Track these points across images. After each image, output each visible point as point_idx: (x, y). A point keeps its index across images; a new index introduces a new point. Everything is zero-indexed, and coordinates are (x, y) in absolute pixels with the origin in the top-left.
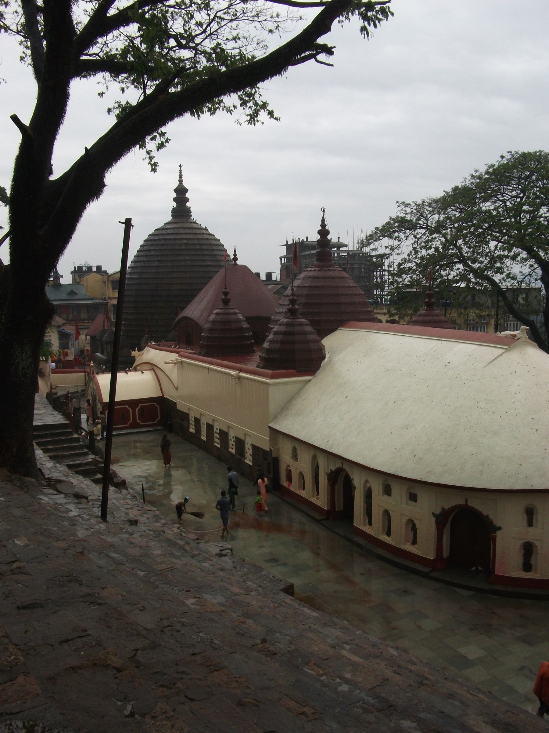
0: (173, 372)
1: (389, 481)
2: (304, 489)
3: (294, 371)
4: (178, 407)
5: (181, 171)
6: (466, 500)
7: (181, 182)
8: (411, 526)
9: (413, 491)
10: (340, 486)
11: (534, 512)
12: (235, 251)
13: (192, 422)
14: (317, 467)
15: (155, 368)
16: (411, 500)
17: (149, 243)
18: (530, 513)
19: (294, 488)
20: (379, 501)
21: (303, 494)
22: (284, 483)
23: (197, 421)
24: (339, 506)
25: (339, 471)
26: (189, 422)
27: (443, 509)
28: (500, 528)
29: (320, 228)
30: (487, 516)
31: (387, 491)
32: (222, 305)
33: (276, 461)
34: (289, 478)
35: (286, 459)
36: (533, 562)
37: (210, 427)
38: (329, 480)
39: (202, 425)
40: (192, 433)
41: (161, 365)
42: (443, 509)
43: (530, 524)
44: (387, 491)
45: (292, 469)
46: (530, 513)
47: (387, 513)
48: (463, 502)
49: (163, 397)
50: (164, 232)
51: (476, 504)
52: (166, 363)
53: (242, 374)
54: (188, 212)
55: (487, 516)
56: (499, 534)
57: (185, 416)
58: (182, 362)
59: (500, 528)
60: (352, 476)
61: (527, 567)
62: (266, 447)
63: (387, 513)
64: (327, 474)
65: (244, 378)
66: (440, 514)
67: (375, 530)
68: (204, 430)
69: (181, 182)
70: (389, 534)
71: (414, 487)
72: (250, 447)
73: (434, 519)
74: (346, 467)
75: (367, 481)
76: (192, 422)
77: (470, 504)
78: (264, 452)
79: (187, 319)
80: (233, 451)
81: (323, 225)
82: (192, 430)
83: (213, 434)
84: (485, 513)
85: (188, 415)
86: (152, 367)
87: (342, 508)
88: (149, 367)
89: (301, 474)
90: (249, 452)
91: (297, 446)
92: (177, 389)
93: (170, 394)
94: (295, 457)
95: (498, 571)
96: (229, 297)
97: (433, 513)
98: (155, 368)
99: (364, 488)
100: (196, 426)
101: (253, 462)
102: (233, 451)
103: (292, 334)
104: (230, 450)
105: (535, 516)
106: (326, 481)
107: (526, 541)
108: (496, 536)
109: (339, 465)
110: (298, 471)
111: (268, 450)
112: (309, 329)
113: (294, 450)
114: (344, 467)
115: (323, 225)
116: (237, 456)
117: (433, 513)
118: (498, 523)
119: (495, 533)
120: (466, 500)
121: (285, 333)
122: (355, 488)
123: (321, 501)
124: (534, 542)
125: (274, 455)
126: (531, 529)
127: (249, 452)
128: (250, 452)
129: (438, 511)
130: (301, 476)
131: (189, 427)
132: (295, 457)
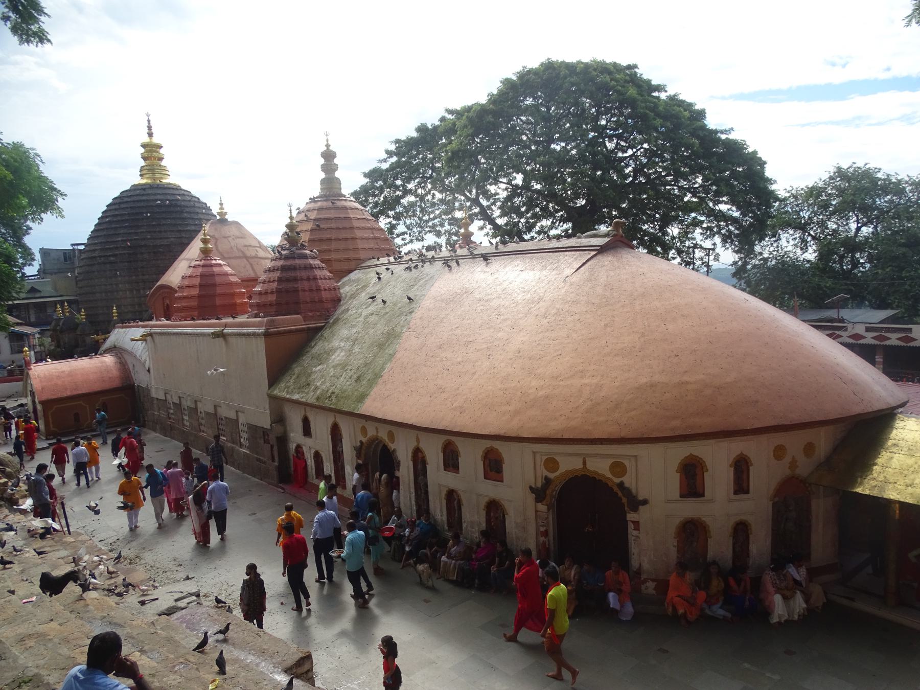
0: (139, 348)
1: (451, 444)
5: (149, 121)
6: (584, 463)
17: (114, 207)
28: (645, 502)
31: (451, 462)
33: (283, 440)
35: (296, 436)
44: (451, 462)
48: (579, 465)
58: (151, 334)
59: (645, 502)
60: (392, 446)
63: (452, 498)
72: (245, 429)
78: (265, 433)
79: (163, 287)
91: (311, 418)
93: (141, 379)
94: (307, 432)
97: (531, 488)
103: (294, 268)
109: (371, 432)
110: (313, 451)
111: (269, 427)
113: (306, 423)
114: (379, 435)
117: (531, 488)
120: (584, 463)
121: (283, 269)
130: (317, 456)
132: (307, 432)
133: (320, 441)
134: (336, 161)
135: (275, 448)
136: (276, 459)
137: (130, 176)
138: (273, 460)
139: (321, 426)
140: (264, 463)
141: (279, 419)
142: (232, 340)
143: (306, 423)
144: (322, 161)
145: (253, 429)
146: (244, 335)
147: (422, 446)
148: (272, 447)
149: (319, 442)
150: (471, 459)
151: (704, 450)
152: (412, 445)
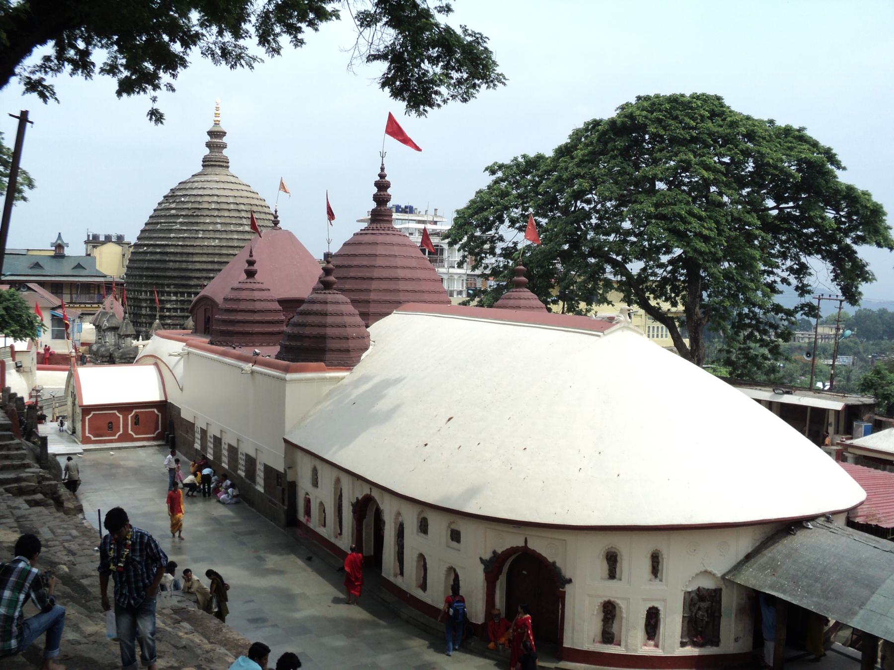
2: (324, 526)
4: (183, 415)
7: (217, 124)
8: (453, 576)
9: (454, 527)
10: (369, 520)
11: (618, 559)
13: (198, 436)
16: (452, 540)
18: (612, 559)
19: (314, 524)
20: (413, 542)
21: (322, 531)
22: (302, 517)
23: (204, 432)
24: (368, 549)
26: (194, 436)
27: (494, 552)
28: (570, 581)
29: (378, 178)
30: (554, 563)
31: (423, 527)
34: (308, 512)
35: (304, 485)
36: (615, 628)
37: (218, 441)
38: (354, 512)
39: (209, 439)
41: (165, 358)
42: (494, 552)
43: (612, 575)
44: (423, 527)
46: (612, 559)
47: (422, 557)
49: (166, 401)
51: (539, 545)
52: (170, 355)
54: (224, 164)
55: (554, 563)
56: (568, 588)
57: (190, 426)
59: (570, 581)
60: (382, 507)
61: (608, 637)
62: (280, 467)
64: (352, 505)
65: (258, 372)
66: (491, 559)
67: (408, 582)
70: (424, 587)
71: (457, 521)
72: (262, 468)
73: (482, 567)
74: (376, 494)
75: (399, 514)
76: (198, 436)
77: (532, 545)
78: (278, 473)
79: (205, 298)
80: (243, 474)
81: (382, 176)
82: (197, 446)
83: (221, 450)
84: (551, 560)
85: (193, 424)
86: (155, 360)
87: (372, 554)
88: (153, 360)
89: (321, 504)
91: (319, 468)
92: (181, 389)
95: (567, 644)
96: (256, 267)
97: (481, 559)
98: (159, 362)
99: (395, 523)
100: (201, 439)
101: (265, 488)
102: (243, 474)
105: (618, 565)
107: (606, 599)
108: (564, 592)
109: (366, 490)
110: (318, 501)
111: (282, 471)
112: (350, 308)
113: (315, 471)
115: (382, 176)
116: (248, 481)
117: (481, 559)
118: (567, 573)
119: (563, 587)
122: (384, 523)
123: (345, 543)
124: (618, 601)
125: (290, 478)
126: (613, 583)
128: (262, 475)
129: (487, 556)
131: (194, 442)
133: (323, 495)
134: (389, 191)
135: (286, 492)
136: (286, 503)
138: (283, 503)
139: (327, 478)
140: (275, 504)
141: (291, 465)
142: (258, 377)
143: (315, 471)
144: (375, 190)
145: (268, 469)
146: (269, 375)
147: (402, 512)
148: (283, 490)
149: (323, 495)
150: (438, 526)
151: (620, 543)
152: (394, 510)
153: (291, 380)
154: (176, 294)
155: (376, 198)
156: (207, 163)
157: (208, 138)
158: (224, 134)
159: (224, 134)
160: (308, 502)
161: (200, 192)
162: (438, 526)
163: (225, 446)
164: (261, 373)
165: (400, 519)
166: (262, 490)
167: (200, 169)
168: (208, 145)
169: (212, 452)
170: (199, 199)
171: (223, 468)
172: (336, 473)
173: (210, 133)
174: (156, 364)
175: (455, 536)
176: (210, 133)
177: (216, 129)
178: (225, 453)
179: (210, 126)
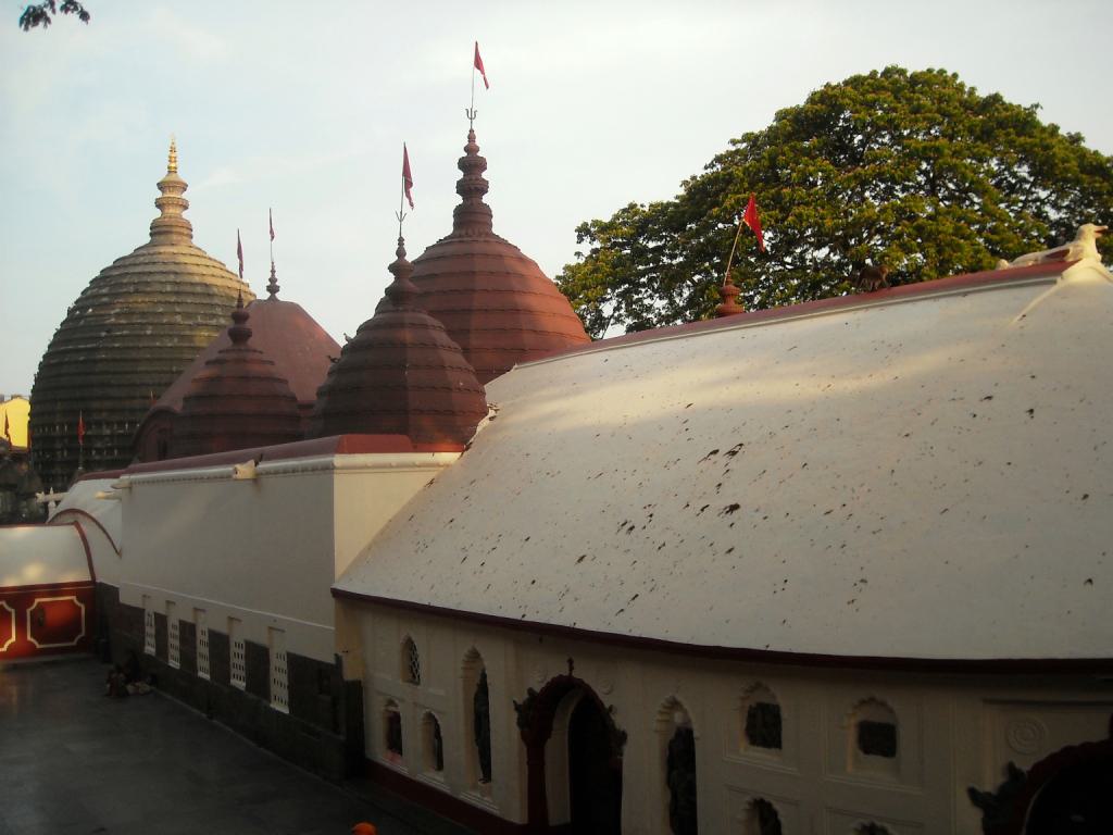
2: (440, 766)
3: (405, 438)
4: (124, 599)
10: (557, 748)
12: (273, 271)
13: (150, 630)
14: (483, 691)
15: (81, 518)
16: (867, 752)
19: (411, 763)
22: (379, 753)
23: (161, 620)
25: (562, 688)
31: (764, 728)
32: (228, 343)
34: (395, 742)
37: (188, 630)
38: (523, 723)
40: (149, 656)
44: (764, 728)
45: (402, 710)
49: (93, 582)
50: (131, 260)
53: (263, 466)
57: (137, 614)
64: (517, 708)
65: (268, 473)
66: (1003, 789)
68: (174, 642)
69: (172, 171)
74: (586, 673)
76: (150, 630)
80: (241, 684)
82: (150, 649)
86: (74, 515)
87: (569, 820)
89: (430, 718)
90: (279, 677)
94: (412, 674)
96: (248, 324)
101: (291, 705)
102: (241, 684)
104: (234, 682)
106: (516, 732)
109: (556, 668)
110: (422, 713)
111: (331, 660)
112: (442, 338)
114: (576, 674)
116: (251, 696)
122: (622, 737)
125: (349, 675)
127: (279, 677)
128: (283, 678)
129: (990, 782)
132: (412, 674)
137: (129, 235)
139: (443, 658)
145: (297, 664)
153: (343, 468)
154: (109, 424)
155: (462, 188)
156: (158, 230)
157: (159, 194)
158: (184, 187)
159: (184, 187)
160: (394, 721)
161: (148, 269)
162: (820, 724)
163: (202, 638)
164: (276, 472)
165: (678, 718)
166: (286, 710)
167: (148, 239)
168: (160, 204)
169: (176, 654)
170: (145, 278)
171: (202, 680)
172: (463, 644)
173: (161, 186)
174: (77, 524)
175: (878, 739)
176: (161, 186)
177: (173, 177)
178: (203, 650)
179: (162, 175)
